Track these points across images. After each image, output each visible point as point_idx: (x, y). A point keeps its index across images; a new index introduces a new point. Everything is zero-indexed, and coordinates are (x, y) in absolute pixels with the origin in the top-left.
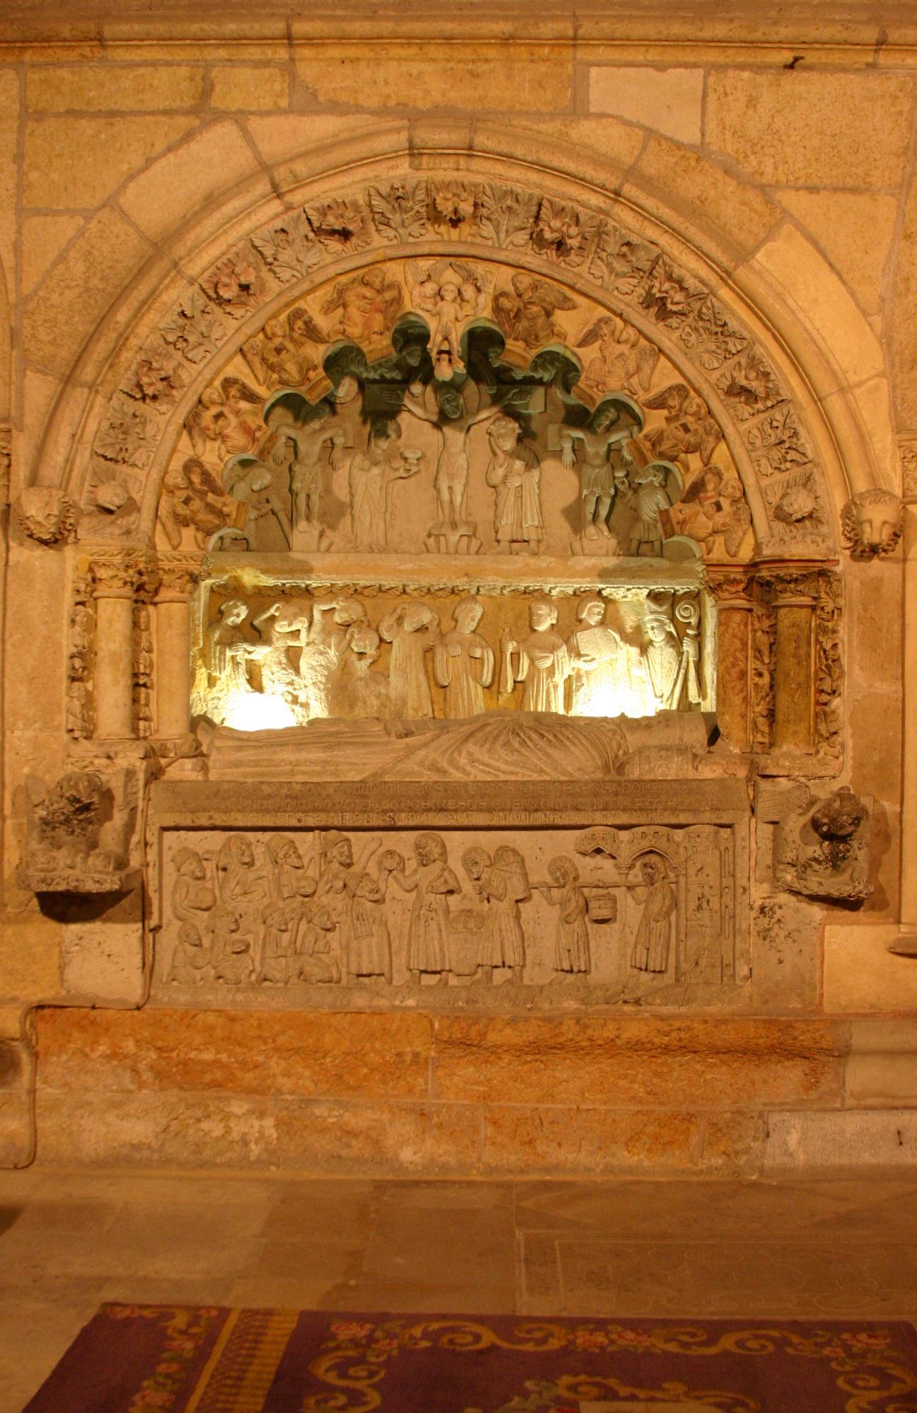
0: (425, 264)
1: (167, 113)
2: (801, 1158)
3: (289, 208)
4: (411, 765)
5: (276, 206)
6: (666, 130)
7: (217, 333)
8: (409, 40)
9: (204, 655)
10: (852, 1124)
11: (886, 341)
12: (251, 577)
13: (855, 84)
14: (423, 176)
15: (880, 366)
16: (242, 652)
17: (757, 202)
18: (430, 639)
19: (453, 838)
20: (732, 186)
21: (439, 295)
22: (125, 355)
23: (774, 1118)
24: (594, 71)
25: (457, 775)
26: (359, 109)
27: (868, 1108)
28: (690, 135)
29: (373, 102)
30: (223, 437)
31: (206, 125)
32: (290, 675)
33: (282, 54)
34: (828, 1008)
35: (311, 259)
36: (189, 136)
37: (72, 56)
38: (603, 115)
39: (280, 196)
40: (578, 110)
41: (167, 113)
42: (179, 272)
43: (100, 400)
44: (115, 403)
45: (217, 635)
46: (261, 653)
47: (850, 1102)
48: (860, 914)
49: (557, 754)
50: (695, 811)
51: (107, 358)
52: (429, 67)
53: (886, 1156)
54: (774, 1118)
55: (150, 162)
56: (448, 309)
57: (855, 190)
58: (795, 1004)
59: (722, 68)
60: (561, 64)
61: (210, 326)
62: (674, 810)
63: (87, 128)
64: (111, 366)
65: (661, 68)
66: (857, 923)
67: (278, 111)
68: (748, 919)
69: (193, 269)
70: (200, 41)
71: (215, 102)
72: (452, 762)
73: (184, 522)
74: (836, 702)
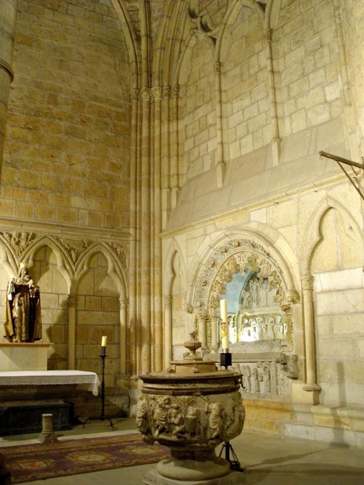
0: (238, 254)
1: (201, 236)
2: (291, 435)
3: (215, 250)
4: (242, 350)
5: (213, 250)
6: (261, 221)
7: (213, 273)
8: (226, 215)
9: (241, 329)
10: (299, 428)
11: (297, 256)
12: (248, 314)
13: (288, 203)
14: (230, 239)
15: (297, 261)
16: (247, 329)
17: (275, 231)
18: (273, 324)
19: (241, 364)
20: (271, 230)
21: (240, 260)
22: (197, 280)
23: (286, 425)
24: (251, 213)
25: (248, 352)
26: (223, 229)
27: (301, 425)
28: (265, 222)
29: (224, 227)
30: (215, 291)
31: (206, 236)
32: (254, 333)
33: (213, 222)
34: (294, 401)
35: (224, 257)
36: (204, 239)
37: (190, 229)
38: (253, 221)
39: (212, 248)
40: (249, 221)
41: (201, 236)
42: (202, 264)
43: (195, 288)
44: (197, 288)
45: (243, 326)
46: (249, 328)
47: (298, 423)
48: (298, 381)
49: (261, 348)
50: (271, 359)
51: (193, 281)
52: (230, 219)
53: (303, 436)
54: (286, 425)
55: (200, 245)
56: (242, 262)
57: (290, 225)
58: (288, 400)
59: (268, 207)
60: (247, 213)
61: (211, 271)
62: (268, 359)
63: (193, 240)
64: (195, 282)
65: (260, 209)
66: (297, 383)
67: (214, 232)
68: (280, 382)
69: (204, 263)
70: (202, 223)
71: (207, 233)
72: (247, 349)
73: (212, 307)
74: (292, 335)
